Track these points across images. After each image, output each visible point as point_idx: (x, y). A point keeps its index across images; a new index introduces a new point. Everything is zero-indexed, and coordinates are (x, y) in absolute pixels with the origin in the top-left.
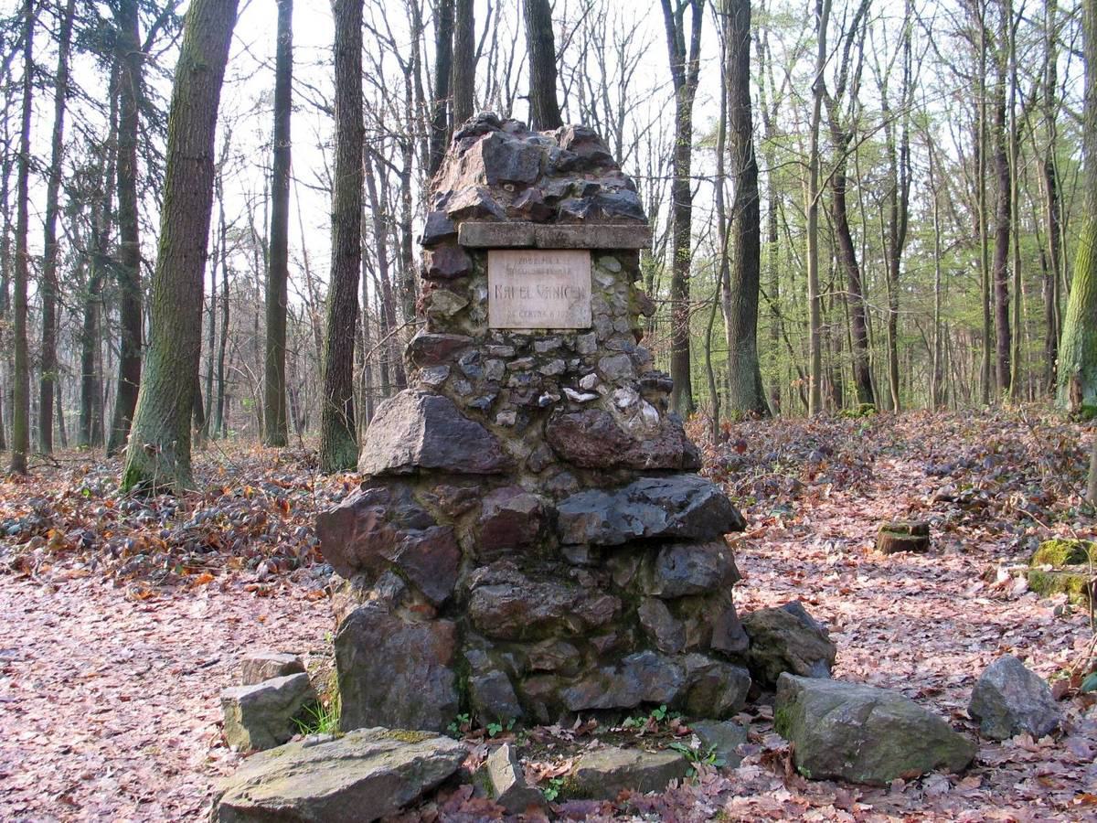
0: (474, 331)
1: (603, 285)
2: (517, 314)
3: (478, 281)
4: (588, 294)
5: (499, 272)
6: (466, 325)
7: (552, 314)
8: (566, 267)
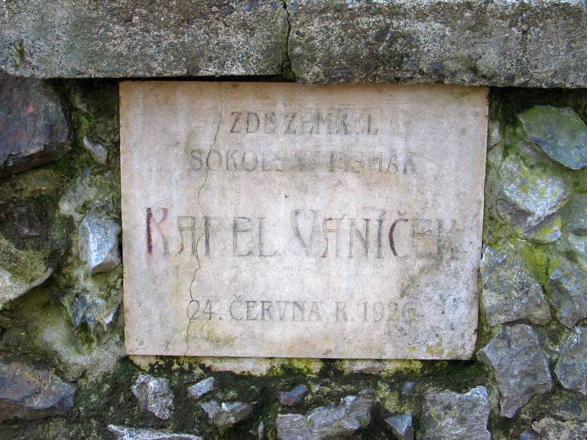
0: (76, 359)
1: (526, 214)
2: (220, 308)
3: (87, 190)
4: (471, 243)
5: (157, 163)
6: (54, 335)
7: (340, 312)
8: (400, 145)
